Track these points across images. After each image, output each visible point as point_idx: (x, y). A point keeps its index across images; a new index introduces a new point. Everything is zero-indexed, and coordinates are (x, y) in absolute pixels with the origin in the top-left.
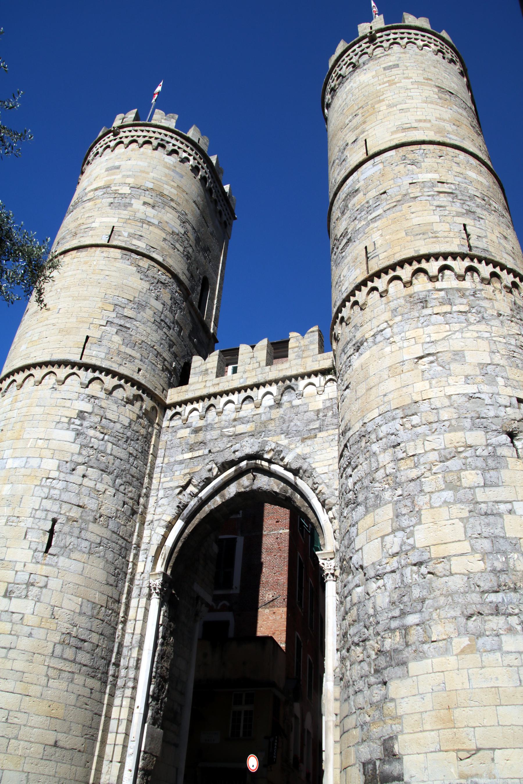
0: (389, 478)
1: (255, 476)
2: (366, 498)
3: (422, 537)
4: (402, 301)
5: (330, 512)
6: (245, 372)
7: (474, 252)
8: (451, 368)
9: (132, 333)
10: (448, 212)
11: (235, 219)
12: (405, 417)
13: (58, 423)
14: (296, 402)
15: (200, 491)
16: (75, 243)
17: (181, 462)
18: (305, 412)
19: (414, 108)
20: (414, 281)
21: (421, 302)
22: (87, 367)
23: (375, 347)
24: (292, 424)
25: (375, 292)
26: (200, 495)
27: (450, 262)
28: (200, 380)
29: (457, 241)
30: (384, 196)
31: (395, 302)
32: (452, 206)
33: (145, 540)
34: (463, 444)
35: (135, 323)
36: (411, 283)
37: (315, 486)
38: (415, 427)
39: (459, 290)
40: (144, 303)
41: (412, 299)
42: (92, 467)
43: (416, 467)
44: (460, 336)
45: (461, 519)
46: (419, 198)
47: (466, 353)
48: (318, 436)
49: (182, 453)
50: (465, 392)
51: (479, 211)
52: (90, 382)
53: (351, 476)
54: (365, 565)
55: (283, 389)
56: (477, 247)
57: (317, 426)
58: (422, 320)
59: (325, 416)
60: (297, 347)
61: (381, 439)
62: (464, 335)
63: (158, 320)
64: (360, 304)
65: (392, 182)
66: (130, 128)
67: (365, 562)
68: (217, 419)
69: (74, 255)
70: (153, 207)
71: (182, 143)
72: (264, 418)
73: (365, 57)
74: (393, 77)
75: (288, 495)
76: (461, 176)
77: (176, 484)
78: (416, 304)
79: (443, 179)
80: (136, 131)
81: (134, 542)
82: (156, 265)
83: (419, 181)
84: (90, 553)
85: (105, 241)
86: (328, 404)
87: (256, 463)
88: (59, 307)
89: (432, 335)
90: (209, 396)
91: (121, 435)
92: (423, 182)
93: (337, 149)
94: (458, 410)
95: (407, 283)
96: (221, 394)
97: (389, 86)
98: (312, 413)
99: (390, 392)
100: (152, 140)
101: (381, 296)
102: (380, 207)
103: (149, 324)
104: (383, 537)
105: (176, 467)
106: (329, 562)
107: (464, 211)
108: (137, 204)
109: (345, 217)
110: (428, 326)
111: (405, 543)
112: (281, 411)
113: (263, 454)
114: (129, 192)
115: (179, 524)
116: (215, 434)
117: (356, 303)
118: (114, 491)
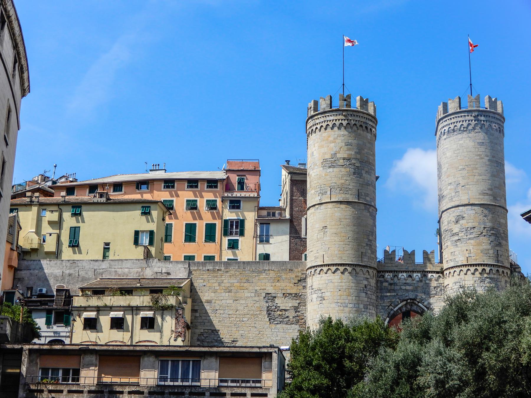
1: (412, 305)
17: (387, 296)
27: (492, 268)
68: (398, 282)
72: (416, 285)
73: (470, 127)
77: (385, 305)
90: (394, 271)
96: (399, 271)
100: (362, 124)
102: (474, 234)
105: (385, 298)
115: (388, 319)
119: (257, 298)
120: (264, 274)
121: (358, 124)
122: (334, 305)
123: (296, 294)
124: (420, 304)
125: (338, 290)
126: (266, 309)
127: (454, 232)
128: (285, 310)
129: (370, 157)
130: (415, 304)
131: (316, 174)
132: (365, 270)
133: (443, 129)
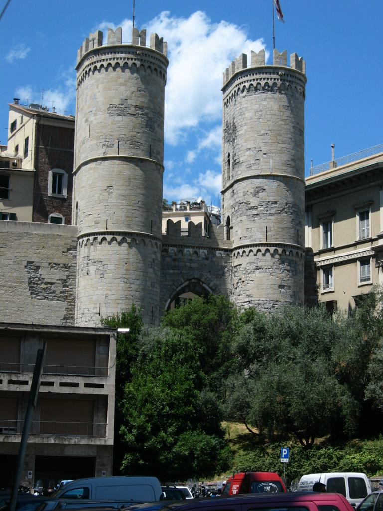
14: (214, 260)
49: (168, 270)
90: (179, 245)
96: (184, 246)
97: (285, 125)
102: (276, 209)
112: (209, 262)
119: (16, 267)
120: (26, 238)
121: (153, 67)
122: (118, 281)
123: (65, 265)
124: (204, 285)
125: (124, 264)
126: (27, 280)
127: (252, 205)
128: (52, 284)
131: (99, 121)
132: (154, 241)
133: (242, 85)
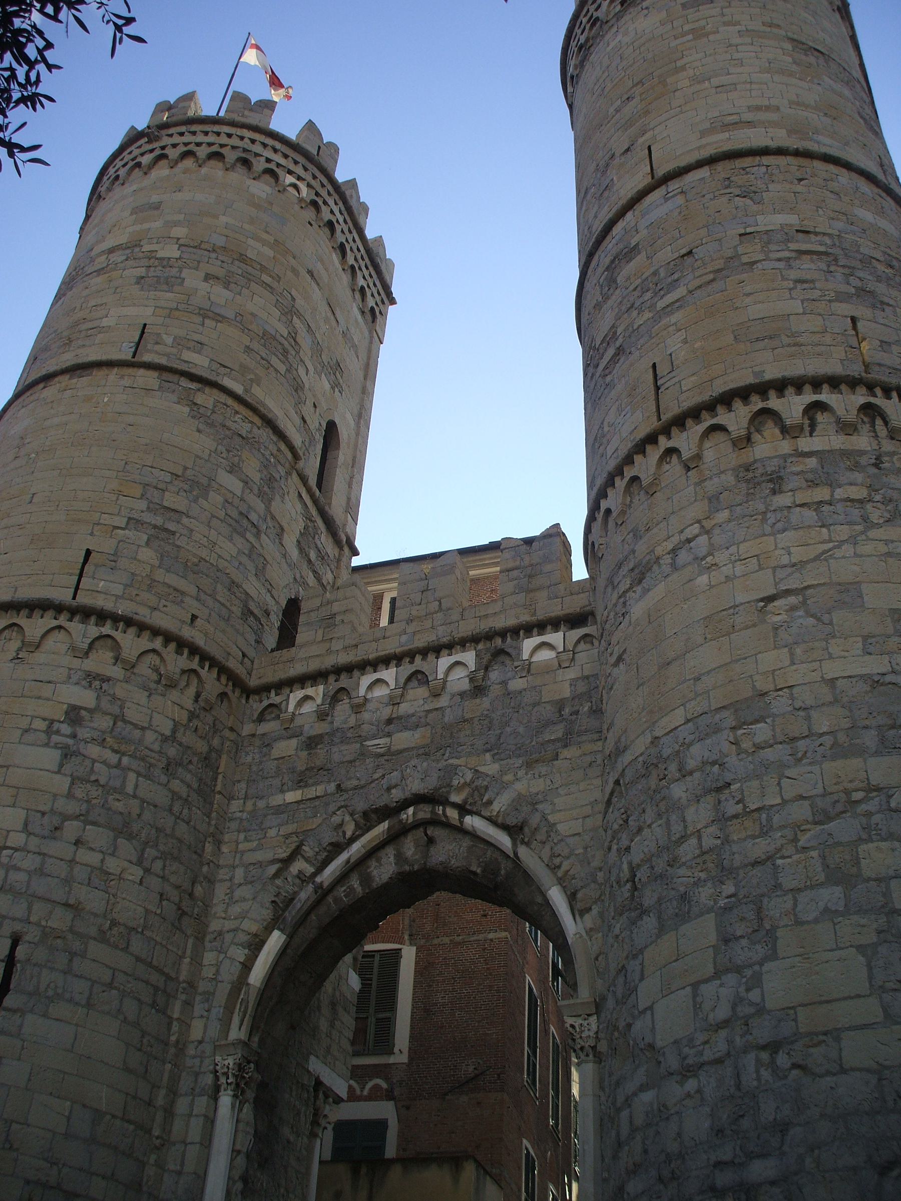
0: (706, 857)
1: (431, 841)
2: (660, 900)
3: (778, 986)
4: (729, 479)
5: (587, 917)
6: (410, 621)
7: (876, 375)
8: (835, 621)
9: (178, 543)
10: (820, 293)
11: (393, 301)
12: (740, 728)
13: (26, 731)
14: (517, 684)
15: (320, 870)
16: (68, 359)
18: (535, 705)
19: (745, 82)
20: (756, 437)
21: (770, 481)
22: (86, 613)
23: (675, 576)
24: (508, 729)
25: (675, 457)
26: (318, 879)
27: (825, 396)
28: (319, 638)
29: (839, 352)
30: (689, 260)
31: (716, 480)
32: (827, 280)
33: (208, 972)
34: (861, 785)
35: (185, 520)
36: (749, 439)
37: (557, 861)
38: (763, 748)
39: (845, 454)
40: (204, 481)
41: (751, 475)
42: (94, 823)
43: (765, 832)
44: (851, 552)
45: (860, 948)
46: (759, 265)
47: (865, 588)
48: (561, 756)
49: (282, 791)
50: (864, 671)
51: (881, 289)
52: (91, 645)
53: (628, 849)
54: (659, 1044)
55: (488, 657)
56: (880, 365)
57: (560, 735)
58: (771, 518)
59: (577, 713)
60: (516, 568)
61: (691, 773)
62: (861, 549)
63: (234, 514)
64: (644, 483)
65: (703, 232)
66: (183, 129)
67: (658, 1037)
69: (63, 384)
70: (227, 285)
71: (286, 156)
72: (449, 717)
74: (703, 23)
75: (499, 879)
76: (844, 218)
77: (269, 856)
78: (759, 484)
79: (808, 225)
80: (194, 133)
81: (181, 979)
82: (230, 401)
83: (758, 229)
84: (89, 1005)
85: (126, 354)
86: (581, 688)
87: (433, 812)
88: (33, 491)
89: (792, 550)
90: (338, 671)
91: (153, 755)
92: (767, 232)
93: (592, 167)
94: (851, 711)
95: (740, 439)
97: (694, 39)
98: (548, 707)
99: (709, 672)
100: (225, 151)
101: (688, 469)
103: (215, 522)
104: (695, 986)
106: (585, 1023)
107: (853, 291)
108: (193, 280)
109: (610, 303)
110: (784, 530)
111: (742, 1000)
112: (485, 703)
113: (449, 793)
114: (177, 254)
115: (276, 940)
116: (348, 751)
117: (635, 479)
118: (141, 873)
124: (471, 821)
129: (251, 242)
130: (447, 825)
